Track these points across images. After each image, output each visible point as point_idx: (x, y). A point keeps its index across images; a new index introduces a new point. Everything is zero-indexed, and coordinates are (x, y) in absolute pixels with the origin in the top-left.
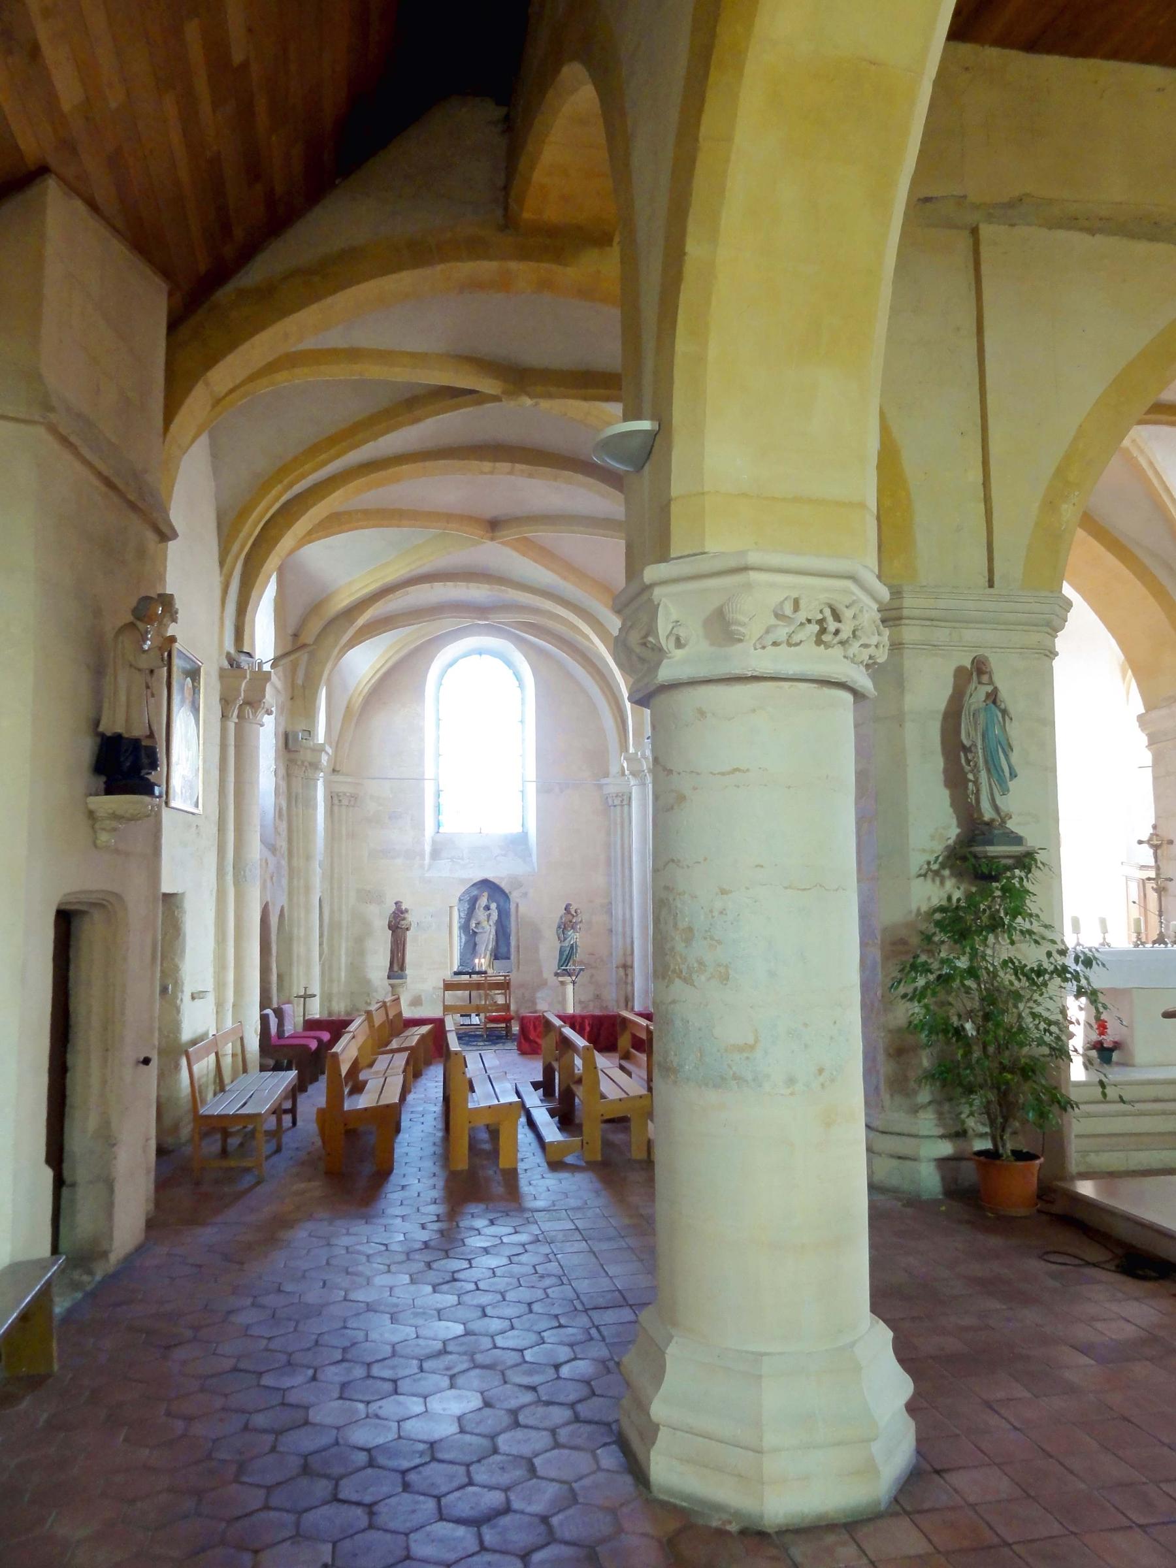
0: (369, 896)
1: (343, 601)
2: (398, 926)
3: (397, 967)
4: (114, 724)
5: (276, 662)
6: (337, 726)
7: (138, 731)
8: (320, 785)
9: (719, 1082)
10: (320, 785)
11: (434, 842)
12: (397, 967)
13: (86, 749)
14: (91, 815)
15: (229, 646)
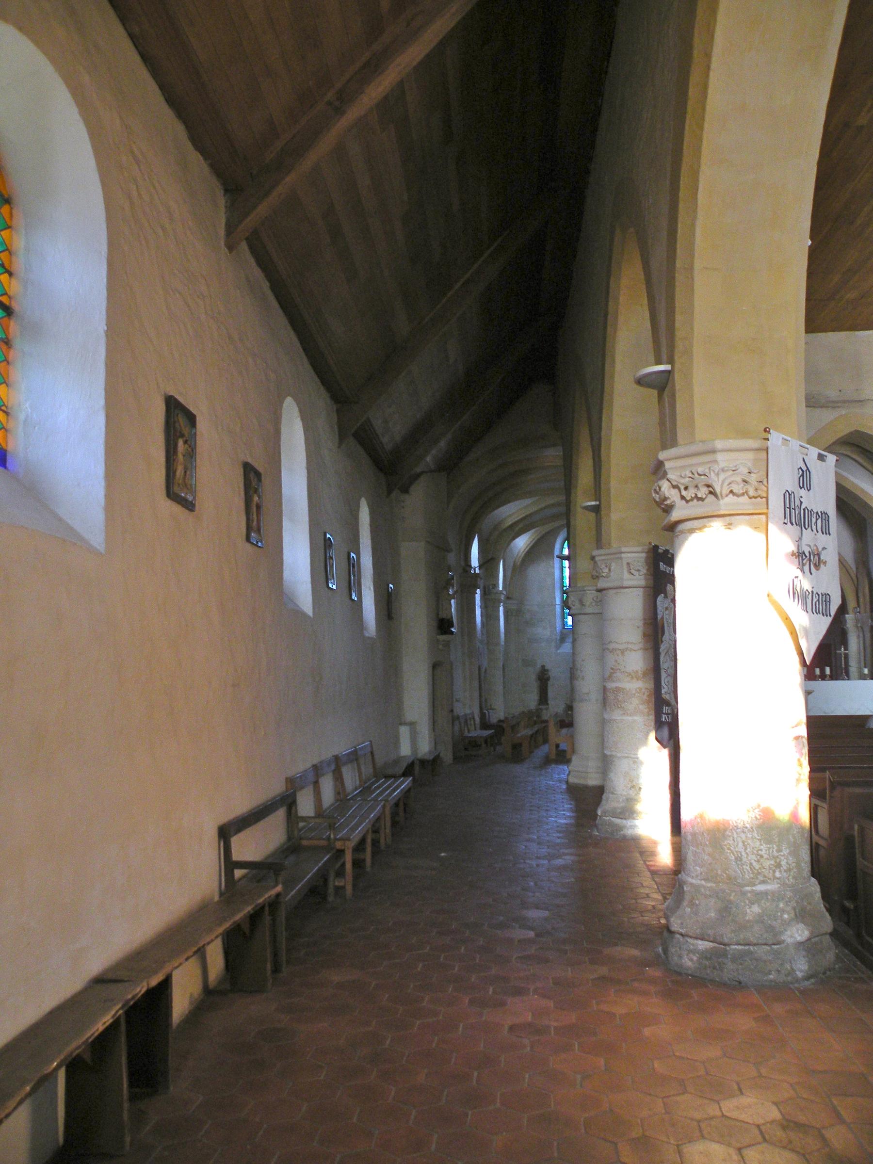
0: (527, 663)
1: (509, 522)
2: (543, 678)
3: (543, 698)
4: (443, 615)
5: (480, 567)
6: (509, 574)
7: (449, 617)
8: (501, 609)
9: (582, 701)
10: (501, 609)
11: (561, 632)
12: (543, 698)
13: (435, 624)
14: (438, 640)
15: (463, 563)
